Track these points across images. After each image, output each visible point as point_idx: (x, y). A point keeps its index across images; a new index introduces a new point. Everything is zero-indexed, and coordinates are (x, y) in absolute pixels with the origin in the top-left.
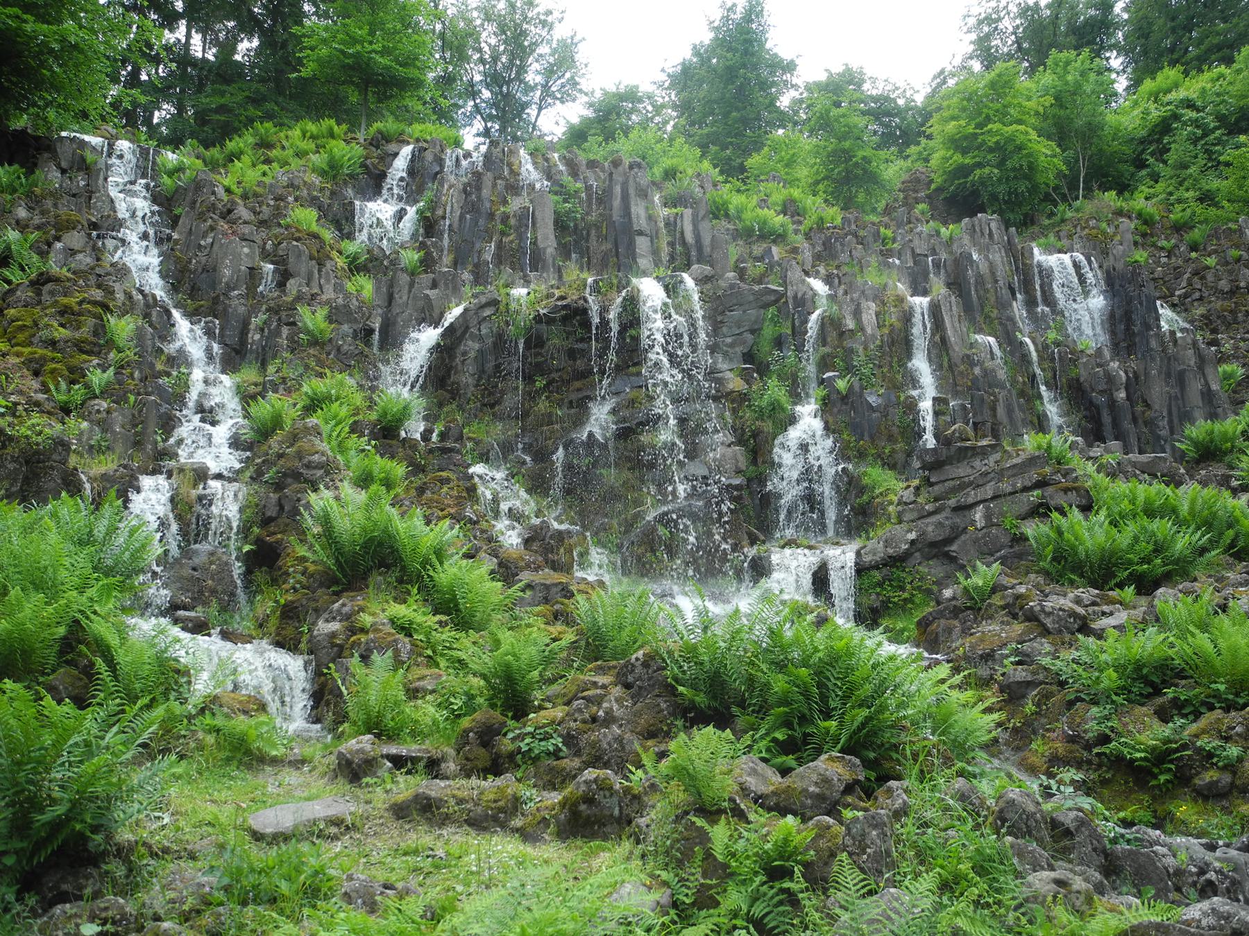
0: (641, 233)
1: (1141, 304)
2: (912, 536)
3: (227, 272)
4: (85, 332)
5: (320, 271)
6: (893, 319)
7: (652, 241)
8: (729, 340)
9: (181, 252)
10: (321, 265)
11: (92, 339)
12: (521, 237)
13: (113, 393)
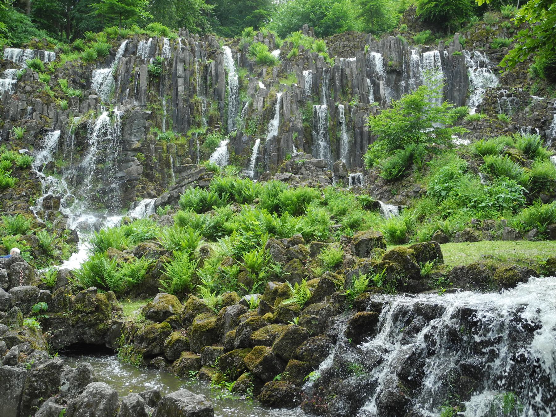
0: (179, 77)
1: (453, 75)
2: (168, 196)
3: (12, 112)
5: (48, 108)
6: (267, 105)
8: (135, 131)
9: (3, 105)
10: (48, 105)
12: (135, 84)
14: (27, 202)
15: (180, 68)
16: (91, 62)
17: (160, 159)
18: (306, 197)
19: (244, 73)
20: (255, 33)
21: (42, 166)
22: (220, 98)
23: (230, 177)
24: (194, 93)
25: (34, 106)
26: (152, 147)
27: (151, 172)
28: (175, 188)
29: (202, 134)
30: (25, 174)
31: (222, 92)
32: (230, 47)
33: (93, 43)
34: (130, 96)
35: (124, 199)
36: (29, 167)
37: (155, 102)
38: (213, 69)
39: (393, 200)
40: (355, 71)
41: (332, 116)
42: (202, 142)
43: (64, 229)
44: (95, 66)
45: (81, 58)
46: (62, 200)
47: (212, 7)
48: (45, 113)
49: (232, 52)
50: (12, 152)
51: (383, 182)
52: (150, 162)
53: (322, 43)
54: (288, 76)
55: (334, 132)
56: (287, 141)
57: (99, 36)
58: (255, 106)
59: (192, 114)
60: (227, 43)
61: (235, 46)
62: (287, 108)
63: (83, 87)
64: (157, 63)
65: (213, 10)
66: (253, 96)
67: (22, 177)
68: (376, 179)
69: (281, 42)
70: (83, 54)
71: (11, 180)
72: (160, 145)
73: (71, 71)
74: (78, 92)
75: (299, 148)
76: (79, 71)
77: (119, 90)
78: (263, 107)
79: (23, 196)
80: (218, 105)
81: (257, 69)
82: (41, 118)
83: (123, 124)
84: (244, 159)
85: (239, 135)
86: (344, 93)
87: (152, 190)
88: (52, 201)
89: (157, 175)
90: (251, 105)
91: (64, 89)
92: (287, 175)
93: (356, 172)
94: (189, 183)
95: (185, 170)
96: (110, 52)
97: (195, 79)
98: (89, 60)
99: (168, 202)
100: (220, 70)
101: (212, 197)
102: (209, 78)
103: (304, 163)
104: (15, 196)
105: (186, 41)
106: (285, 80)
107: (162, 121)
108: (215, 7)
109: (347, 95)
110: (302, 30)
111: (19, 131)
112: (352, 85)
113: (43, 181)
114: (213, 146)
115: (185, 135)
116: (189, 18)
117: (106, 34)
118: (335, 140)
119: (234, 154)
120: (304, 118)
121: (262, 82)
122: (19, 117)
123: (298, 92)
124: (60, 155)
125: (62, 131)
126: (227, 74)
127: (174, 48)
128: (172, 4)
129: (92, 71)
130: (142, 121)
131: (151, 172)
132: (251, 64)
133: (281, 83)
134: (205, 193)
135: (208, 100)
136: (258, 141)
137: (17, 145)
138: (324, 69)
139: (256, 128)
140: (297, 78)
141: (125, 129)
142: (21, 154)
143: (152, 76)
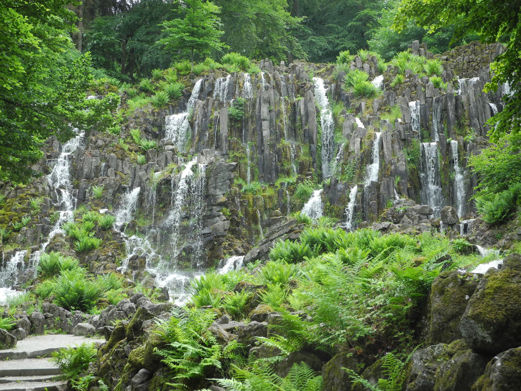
0: (264, 120)
2: (258, 251)
3: (86, 170)
4: (25, 206)
5: (122, 162)
6: (365, 146)
7: (270, 122)
8: (220, 184)
9: (76, 162)
11: (26, 207)
13: (29, 225)
14: (114, 263)
15: (264, 109)
16: (163, 108)
17: (247, 214)
18: (397, 243)
19: (340, 108)
20: (351, 58)
21: (124, 225)
22: (311, 141)
23: (322, 228)
24: (281, 137)
25: (108, 162)
26: (237, 200)
27: (237, 228)
28: (265, 243)
29: (292, 184)
30: (108, 235)
31: (313, 134)
32: (322, 77)
33: (161, 82)
34: (209, 145)
35: (210, 258)
36: (111, 227)
37: (238, 150)
38: (302, 107)
39: (497, 245)
40: (472, 98)
41: (442, 154)
42: (292, 192)
43: (154, 287)
44: (168, 111)
45: (152, 104)
47: (300, 20)
48: (120, 169)
49: (325, 83)
50: (93, 212)
51: (487, 227)
52: (235, 217)
53: (437, 63)
54: (392, 109)
55: (446, 173)
56: (388, 187)
57: (167, 72)
58: (351, 148)
59: (280, 161)
60: (319, 71)
61: (329, 75)
62: (388, 148)
63: (156, 136)
64: (238, 105)
65: (302, 23)
66: (349, 136)
67: (105, 238)
68: (481, 223)
69: (385, 66)
70: (154, 98)
71: (96, 242)
72: (245, 198)
73: (142, 120)
74: (151, 143)
75: (403, 194)
76: (151, 118)
77: (197, 138)
78: (361, 148)
79: (109, 256)
80: (310, 149)
81: (355, 102)
82: (116, 174)
83: (208, 178)
84: (340, 209)
85: (333, 182)
86: (460, 126)
87: (239, 247)
89: (244, 231)
90: (347, 147)
91: (137, 141)
92: (386, 224)
93: (469, 218)
94: (279, 236)
95: (275, 223)
96: (183, 93)
97: (281, 121)
98: (160, 105)
99: (259, 257)
100: (310, 109)
101: (303, 248)
102: (298, 117)
103: (405, 211)
104: (101, 257)
105: (270, 75)
106: (387, 114)
107: (247, 171)
108: (304, 19)
109: (464, 128)
110: (411, 47)
111: (97, 190)
112: (470, 115)
113: (126, 241)
114: (305, 196)
115: (273, 185)
116: (273, 36)
117: (176, 71)
118: (447, 183)
119: (328, 204)
120: (409, 159)
121: (360, 119)
122: (93, 174)
123: (402, 130)
124: (140, 213)
125: (142, 188)
126: (318, 112)
127: (256, 84)
128: (250, 23)
129: (164, 118)
130: (227, 173)
131: (237, 228)
132: (347, 97)
133: (382, 119)
134: (296, 245)
135: (298, 143)
136: (354, 190)
137: (97, 205)
138: (434, 98)
139: (354, 173)
140: (401, 112)
141: (210, 183)
142: (102, 214)
143: (232, 119)
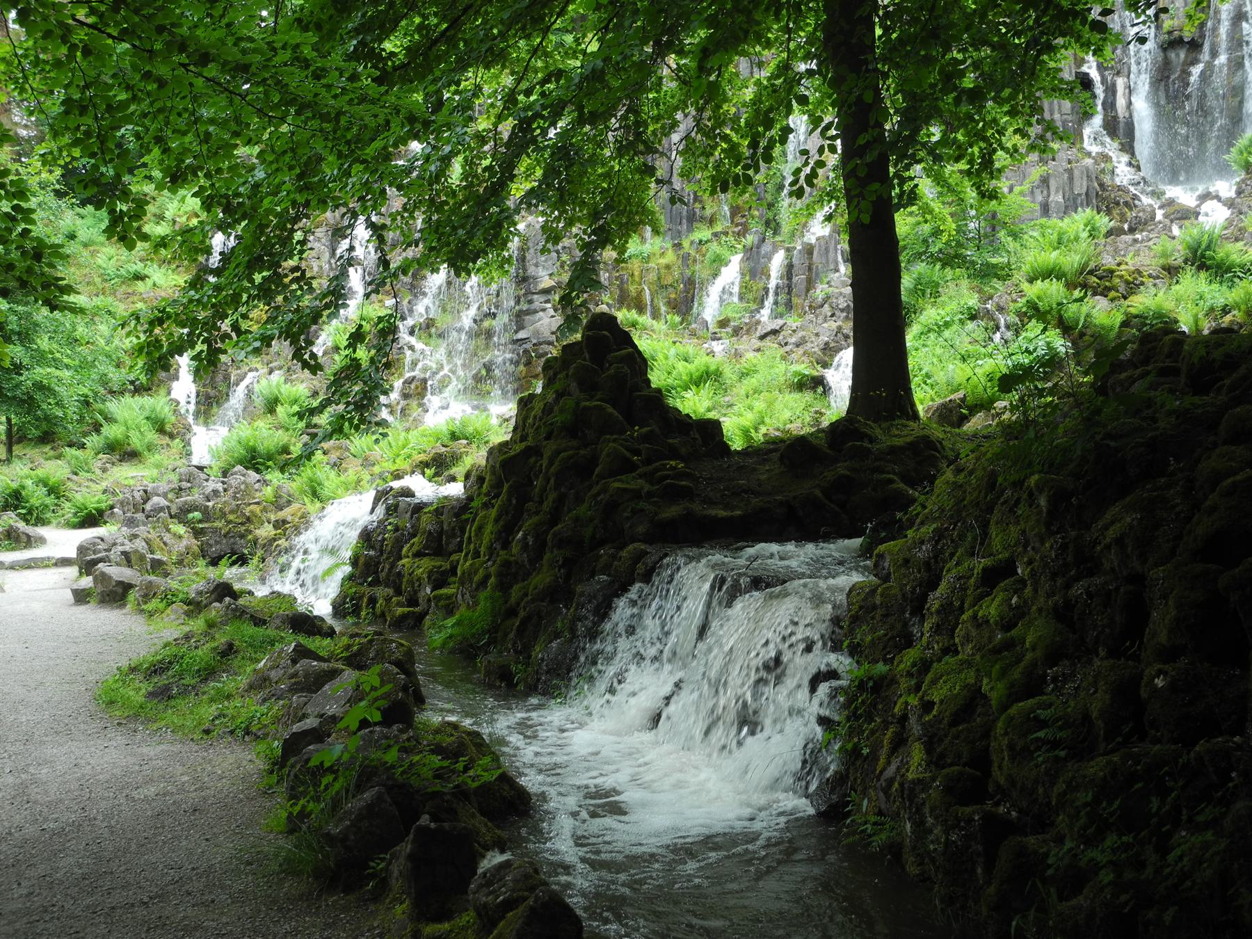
46: (430, 383)
88: (413, 386)
113: (408, 353)
141: (528, 256)
